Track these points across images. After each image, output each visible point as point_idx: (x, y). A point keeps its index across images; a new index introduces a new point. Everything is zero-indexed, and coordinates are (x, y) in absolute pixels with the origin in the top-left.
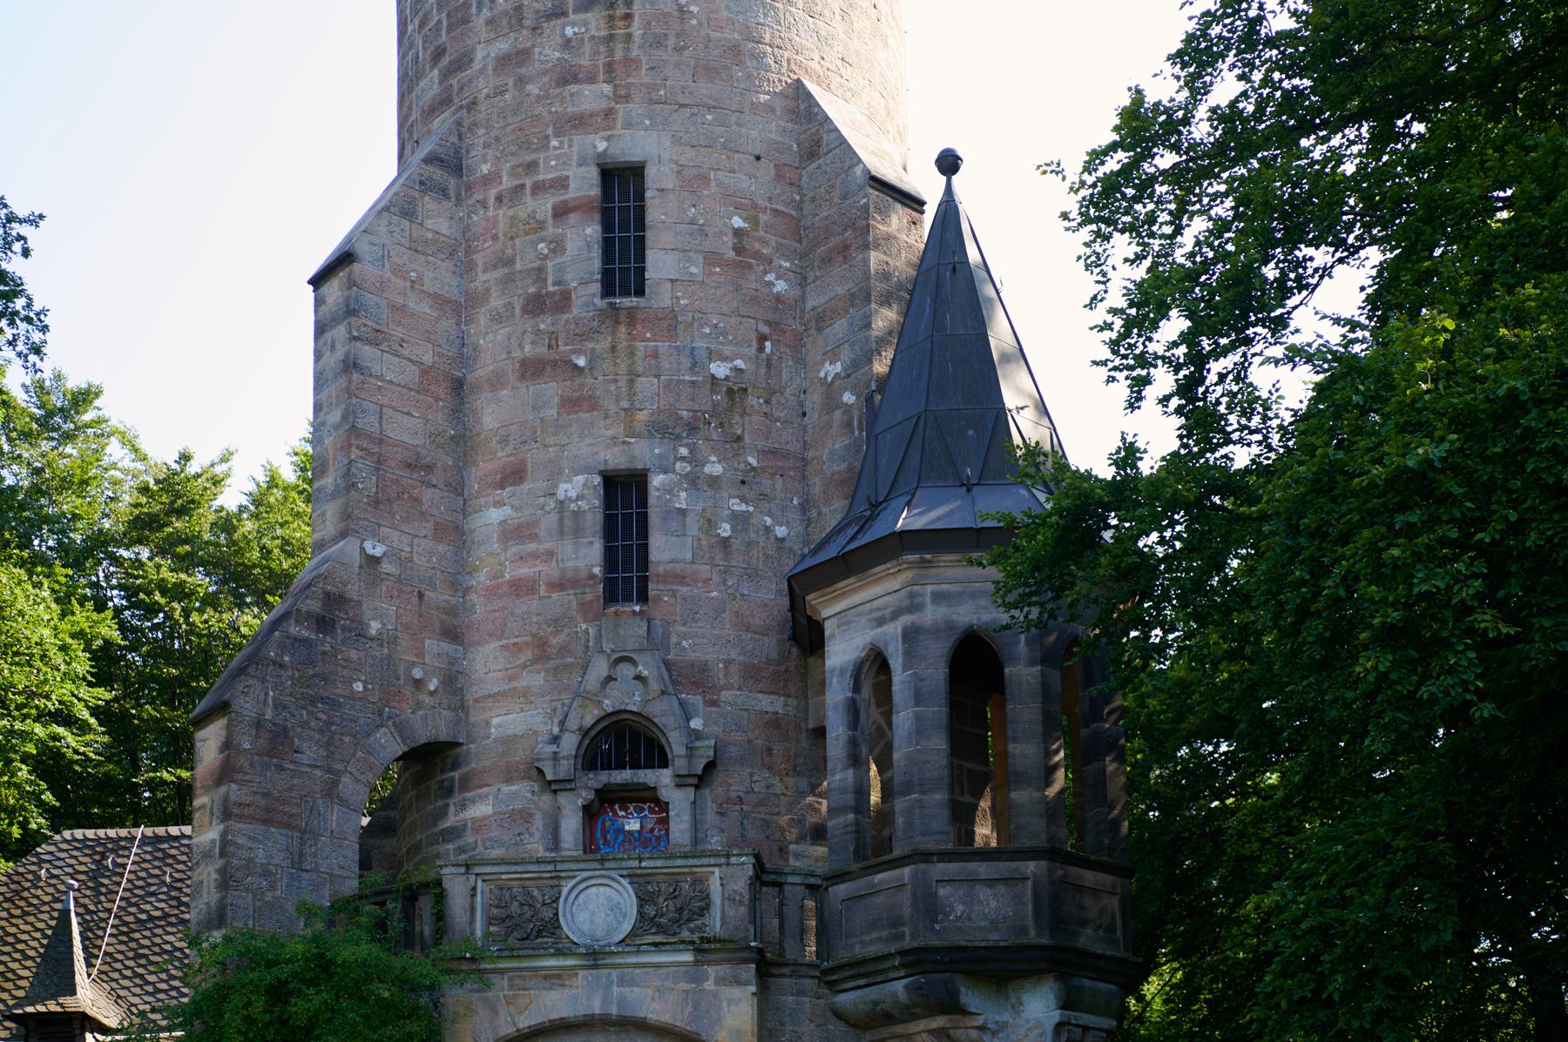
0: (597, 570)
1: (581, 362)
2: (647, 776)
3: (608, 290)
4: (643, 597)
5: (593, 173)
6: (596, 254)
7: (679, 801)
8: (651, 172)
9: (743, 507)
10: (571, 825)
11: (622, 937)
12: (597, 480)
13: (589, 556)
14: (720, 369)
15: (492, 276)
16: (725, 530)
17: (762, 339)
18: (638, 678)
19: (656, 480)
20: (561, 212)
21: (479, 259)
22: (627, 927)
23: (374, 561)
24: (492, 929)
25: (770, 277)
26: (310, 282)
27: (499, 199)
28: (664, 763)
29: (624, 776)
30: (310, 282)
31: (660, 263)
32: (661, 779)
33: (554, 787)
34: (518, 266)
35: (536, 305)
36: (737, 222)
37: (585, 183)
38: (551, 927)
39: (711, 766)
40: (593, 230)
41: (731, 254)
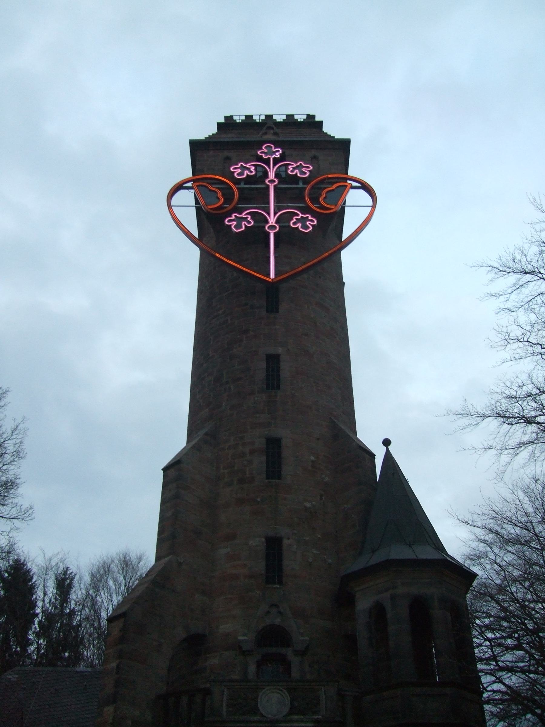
0: (264, 572)
1: (259, 500)
2: (283, 650)
3: (268, 477)
4: (280, 582)
5: (264, 441)
6: (265, 465)
7: (295, 661)
8: (284, 442)
9: (317, 552)
10: (252, 668)
11: (284, 714)
12: (263, 540)
13: (261, 567)
14: (308, 505)
15: (226, 471)
16: (310, 560)
17: (321, 496)
18: (280, 613)
19: (286, 542)
20: (252, 452)
21: (222, 467)
22: (286, 710)
23: (180, 564)
24: (230, 709)
25: (323, 476)
26: (162, 470)
27: (229, 448)
28: (288, 646)
29: (273, 650)
30: (162, 470)
31: (288, 469)
32: (288, 652)
33: (245, 653)
34: (236, 468)
35: (241, 481)
36: (312, 458)
37: (260, 443)
38: (255, 710)
39: (307, 647)
40: (264, 458)
41: (310, 468)
